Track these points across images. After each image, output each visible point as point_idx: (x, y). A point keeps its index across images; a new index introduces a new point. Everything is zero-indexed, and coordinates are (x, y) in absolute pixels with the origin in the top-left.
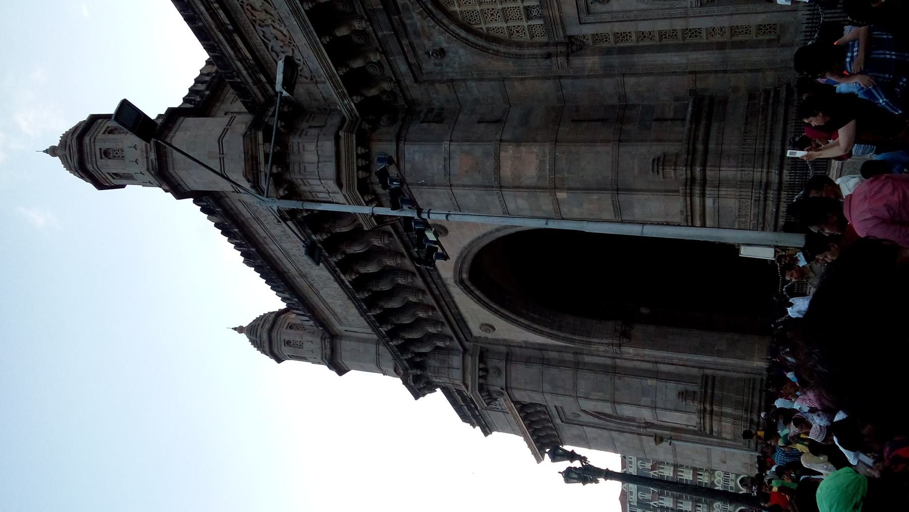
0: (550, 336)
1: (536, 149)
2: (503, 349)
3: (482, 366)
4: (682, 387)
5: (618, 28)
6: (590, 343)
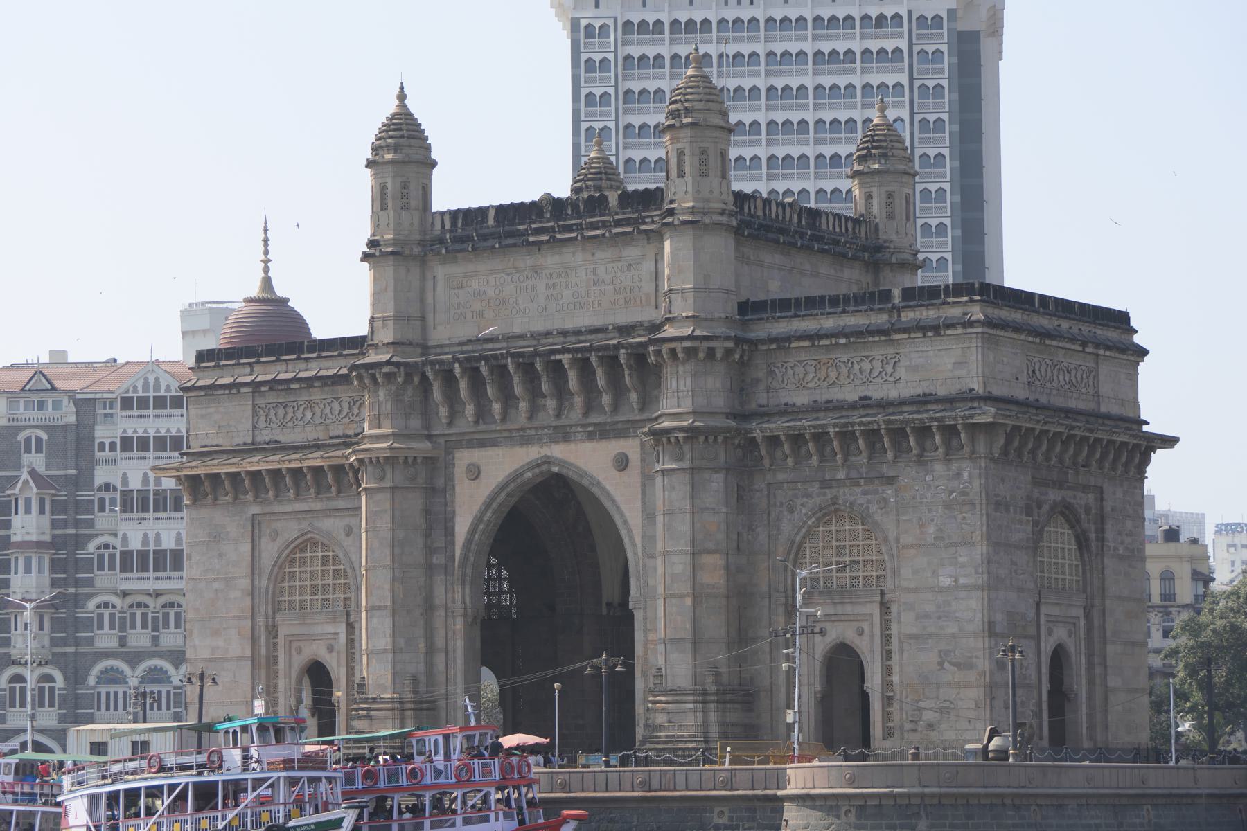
0: (469, 541)
1: (722, 582)
2: (440, 482)
3: (419, 460)
6: (463, 583)
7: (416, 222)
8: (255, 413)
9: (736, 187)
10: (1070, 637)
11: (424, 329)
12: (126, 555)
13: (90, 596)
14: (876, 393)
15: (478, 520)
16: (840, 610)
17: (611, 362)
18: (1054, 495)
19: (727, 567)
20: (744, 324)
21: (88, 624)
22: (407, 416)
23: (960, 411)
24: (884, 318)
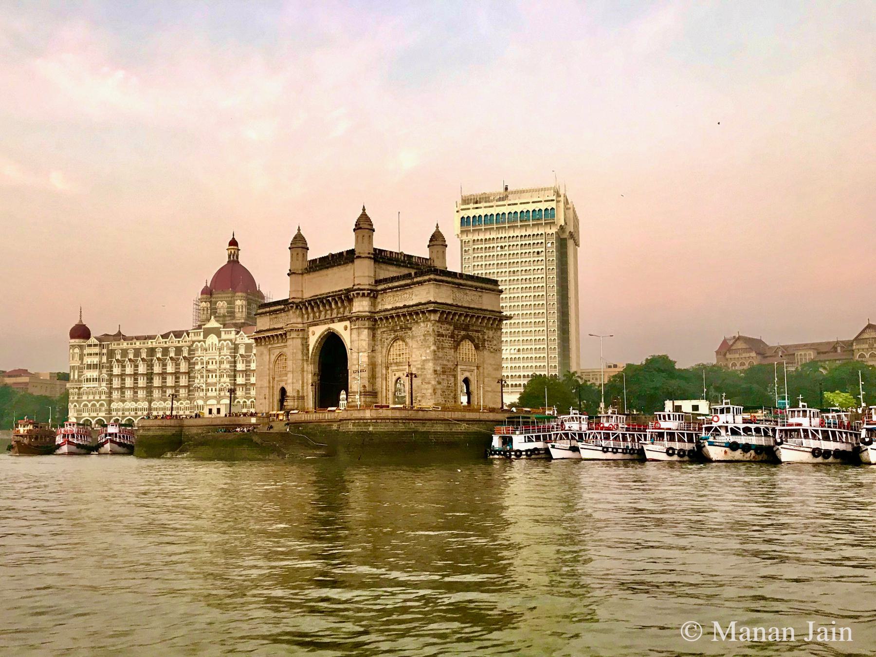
0: (312, 352)
4: (300, 391)
5: (390, 377)
6: (311, 364)
7: (301, 264)
8: (270, 321)
10: (471, 375)
11: (302, 294)
15: (314, 346)
16: (399, 368)
17: (340, 298)
18: (463, 333)
19: (368, 356)
20: (376, 286)
22: (297, 318)
23: (427, 306)
24: (408, 281)
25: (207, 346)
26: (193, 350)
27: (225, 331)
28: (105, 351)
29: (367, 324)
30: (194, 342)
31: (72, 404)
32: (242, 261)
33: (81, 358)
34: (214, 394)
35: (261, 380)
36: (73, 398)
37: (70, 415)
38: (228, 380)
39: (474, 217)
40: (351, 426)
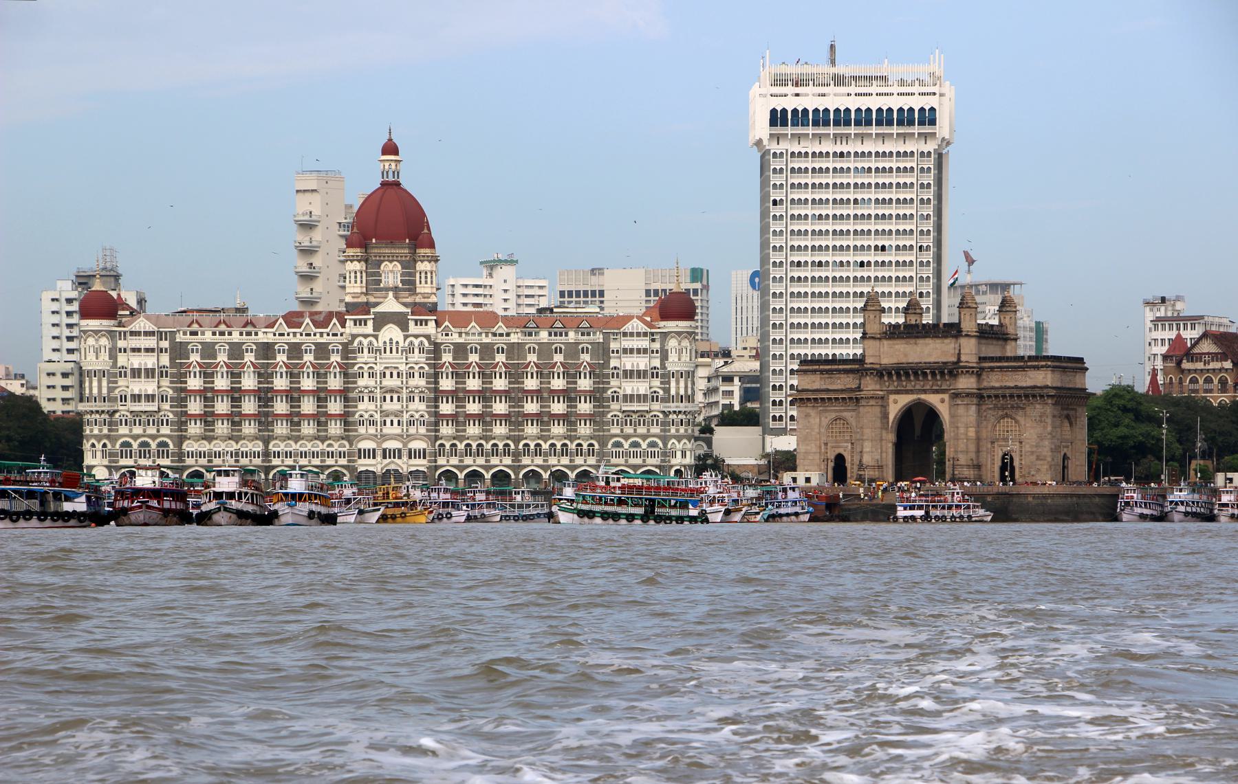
9: (979, 322)
12: (625, 396)
13: (609, 412)
14: (1020, 384)
18: (1065, 412)
21: (607, 423)
23: (1045, 391)
25: (381, 344)
26: (353, 352)
27: (416, 321)
28: (165, 344)
29: (975, 400)
30: (354, 337)
31: (99, 442)
32: (405, 184)
33: (113, 357)
34: (396, 430)
35: (807, 445)
36: (91, 431)
37: (88, 460)
38: (422, 406)
39: (795, 111)
40: (1030, 499)
